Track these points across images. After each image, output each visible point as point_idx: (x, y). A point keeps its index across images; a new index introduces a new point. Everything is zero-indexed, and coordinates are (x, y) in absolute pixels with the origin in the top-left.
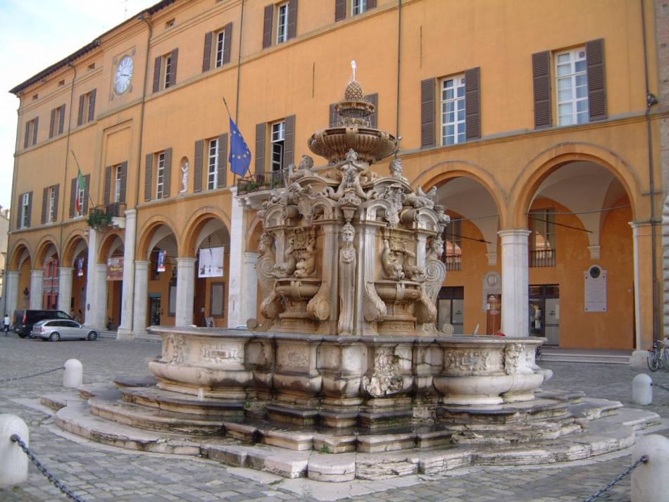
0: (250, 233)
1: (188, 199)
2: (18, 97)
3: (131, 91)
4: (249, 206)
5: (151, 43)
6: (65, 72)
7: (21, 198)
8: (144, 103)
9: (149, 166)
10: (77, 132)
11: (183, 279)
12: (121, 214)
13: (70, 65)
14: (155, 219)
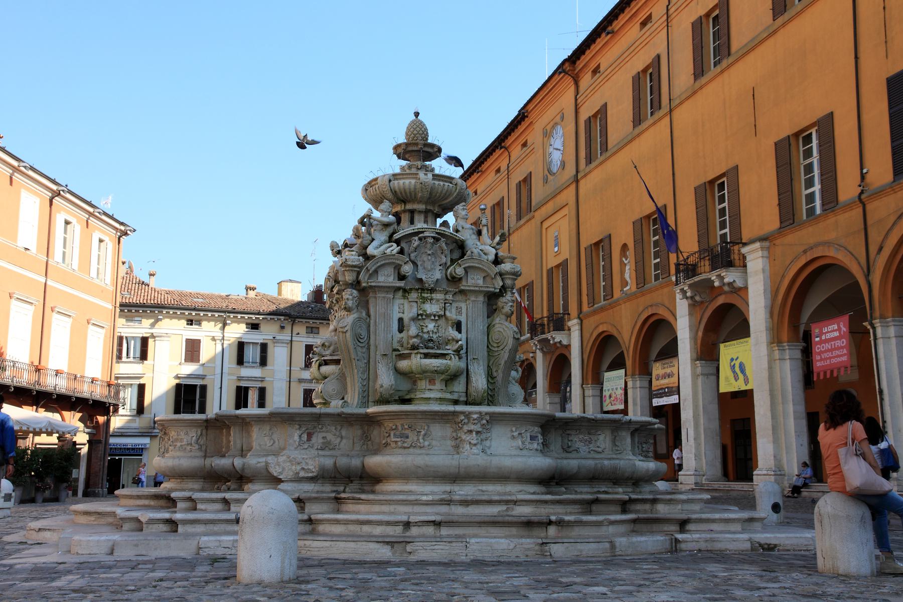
0: (700, 334)
1: (629, 297)
4: (692, 298)
5: (579, 101)
8: (577, 181)
10: (517, 229)
11: (635, 404)
12: (566, 328)
13: (501, 148)
14: (601, 329)
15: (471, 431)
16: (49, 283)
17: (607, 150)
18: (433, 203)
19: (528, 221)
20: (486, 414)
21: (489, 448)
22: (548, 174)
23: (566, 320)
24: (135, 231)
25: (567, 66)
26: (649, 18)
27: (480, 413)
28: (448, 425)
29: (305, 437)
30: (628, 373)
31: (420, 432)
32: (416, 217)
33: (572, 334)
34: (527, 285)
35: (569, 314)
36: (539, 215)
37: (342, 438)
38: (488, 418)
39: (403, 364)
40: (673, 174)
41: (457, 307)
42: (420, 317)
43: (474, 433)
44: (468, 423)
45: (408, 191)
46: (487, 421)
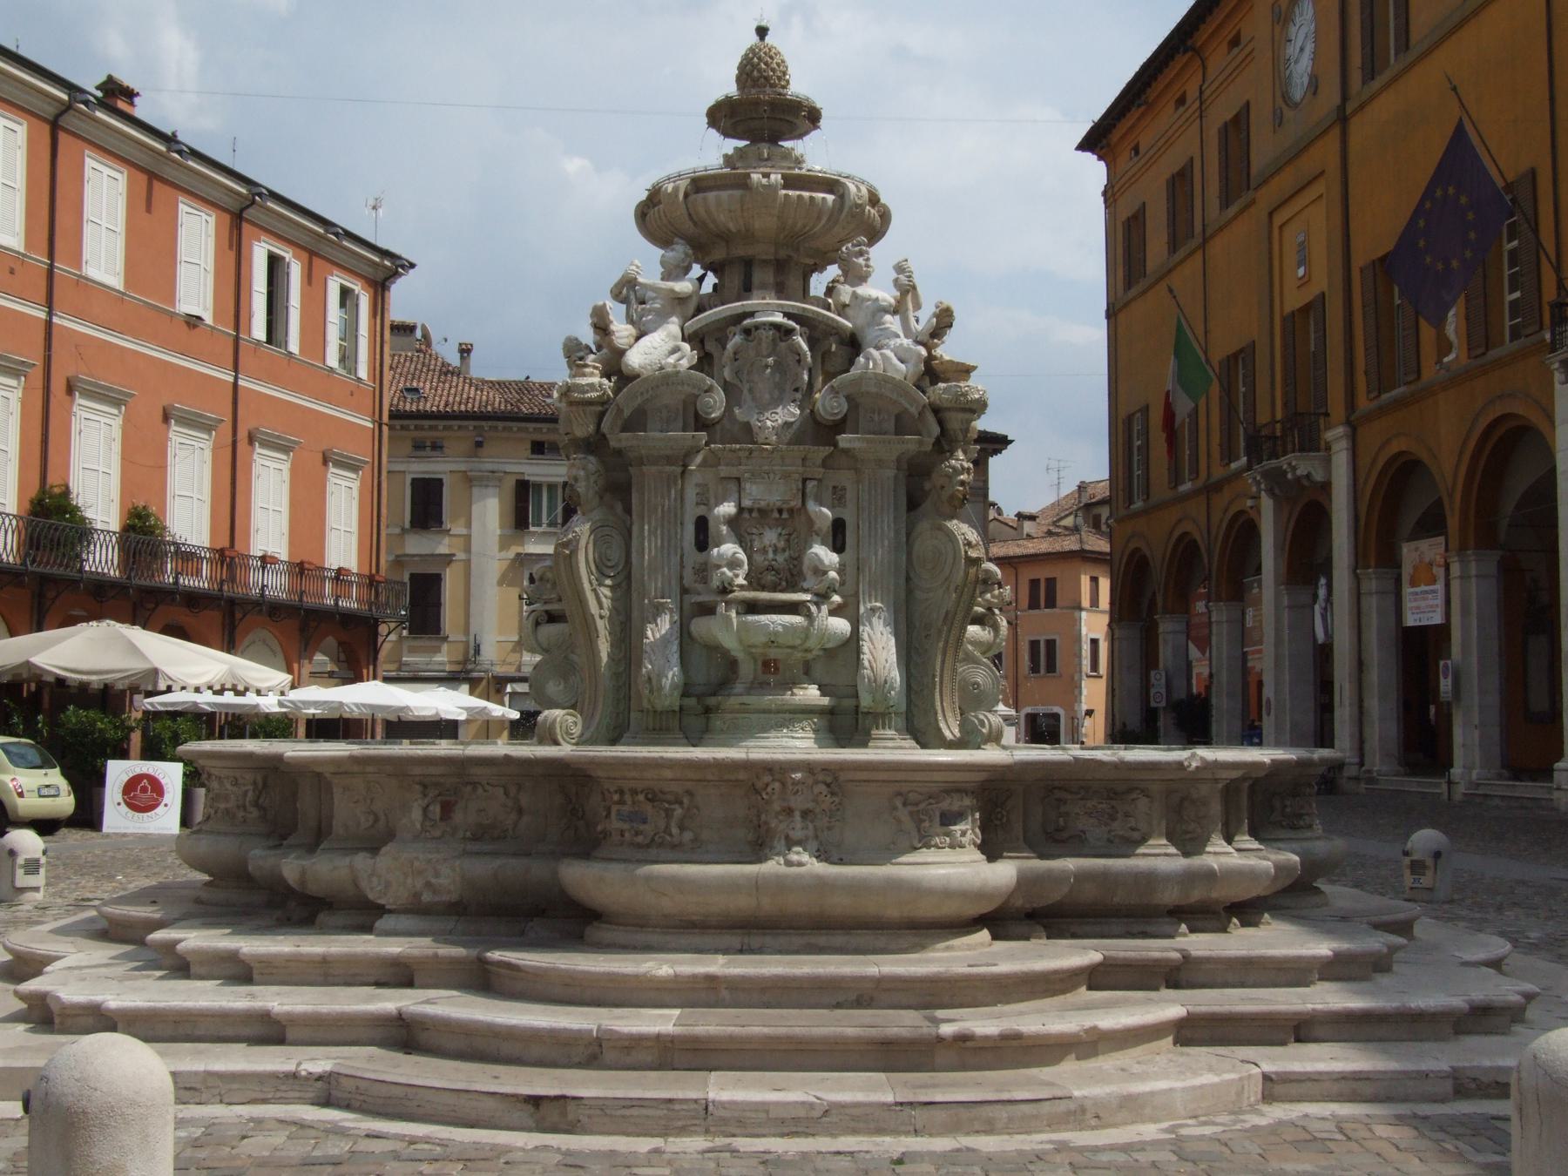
2: (1100, 158)
3: (1315, 93)
6: (1182, 69)
7: (1129, 419)
8: (1342, 119)
10: (1221, 229)
11: (1465, 611)
14: (1396, 447)
17: (1407, 47)
19: (1242, 211)
22: (1284, 106)
23: (1322, 427)
24: (412, 266)
29: (436, 809)
30: (1450, 546)
32: (758, 276)
33: (1334, 458)
34: (1242, 351)
35: (1327, 414)
36: (1267, 196)
37: (520, 811)
40: (1552, 99)
41: (834, 487)
43: (797, 814)
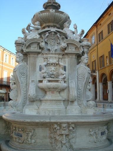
1: (108, 66)
8: (97, 45)
9: (100, 59)
11: (109, 86)
15: (62, 135)
16: (3, 66)
18: (57, 23)
20: (72, 123)
21: (75, 143)
25: (95, 24)
26: (110, 14)
27: (68, 123)
28: (48, 129)
31: (29, 134)
38: (73, 126)
39: (40, 85)
42: (47, 65)
43: (64, 136)
44: (60, 129)
45: (44, 17)
46: (73, 128)
